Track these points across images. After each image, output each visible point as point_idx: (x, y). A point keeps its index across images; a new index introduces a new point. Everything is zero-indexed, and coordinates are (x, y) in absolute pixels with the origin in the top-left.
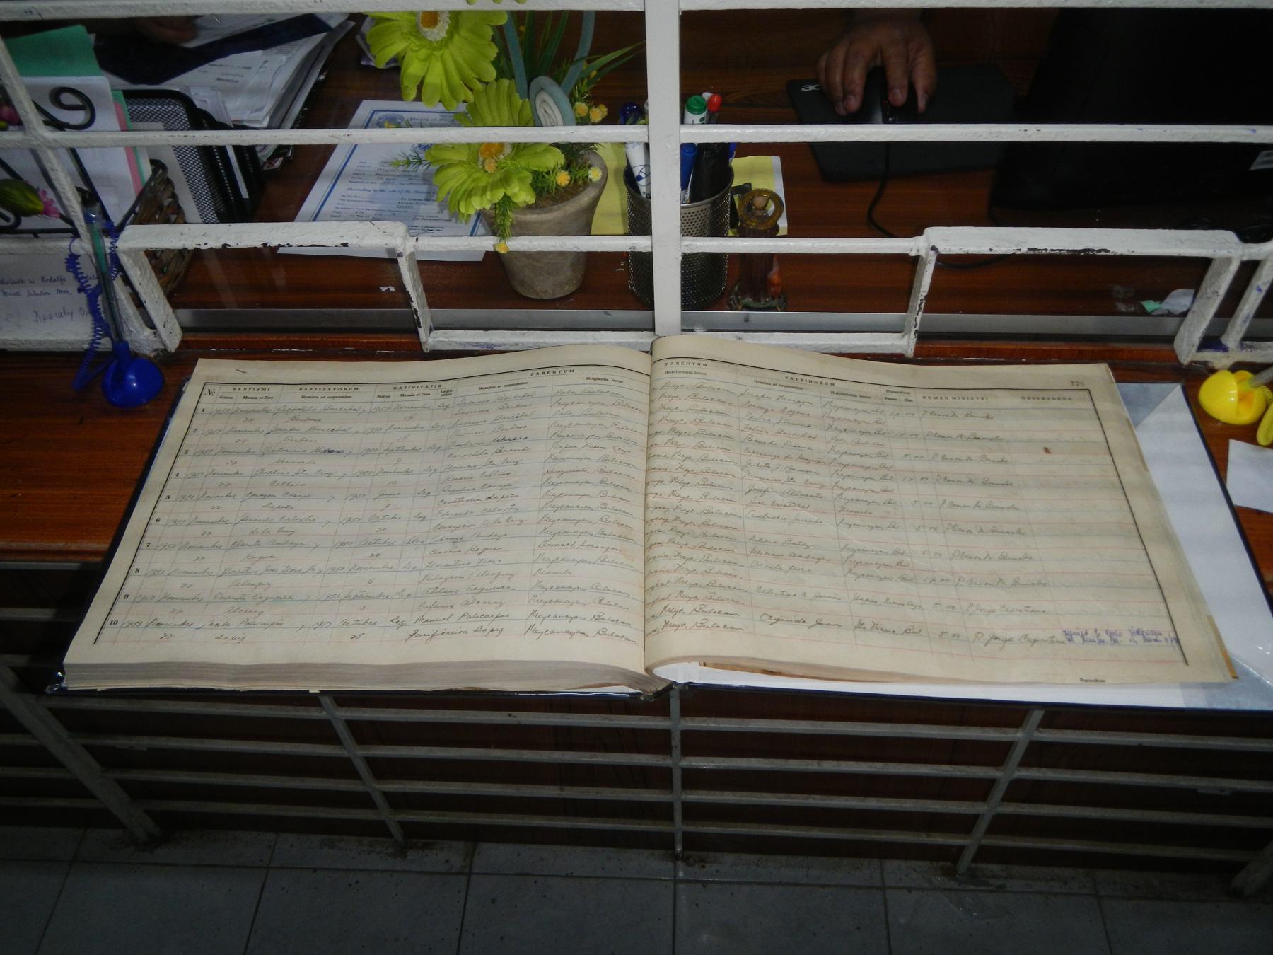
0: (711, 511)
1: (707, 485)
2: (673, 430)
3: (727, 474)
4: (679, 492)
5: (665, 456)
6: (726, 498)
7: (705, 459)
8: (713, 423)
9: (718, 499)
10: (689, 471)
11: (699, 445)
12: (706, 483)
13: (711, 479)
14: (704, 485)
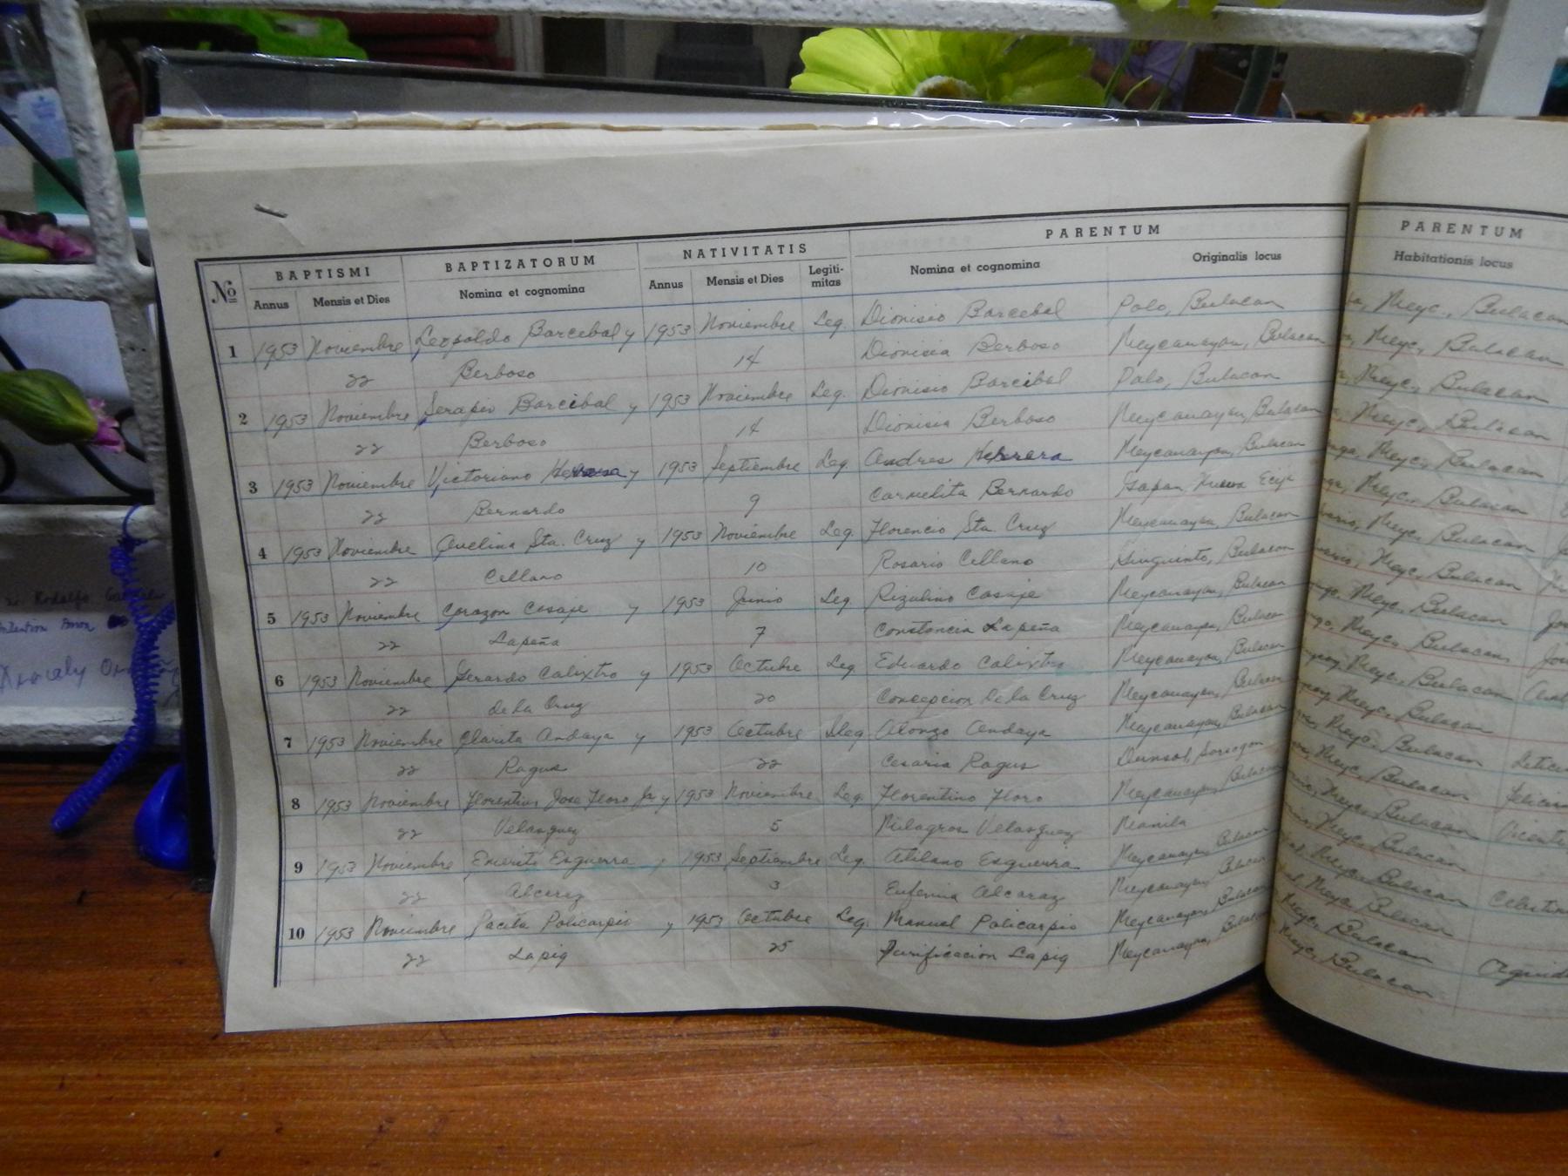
0: (1440, 680)
1: (1444, 612)
2: (1383, 449)
3: (1501, 583)
4: (1367, 624)
5: (1353, 523)
6: (1485, 649)
7: (1453, 539)
8: (1500, 429)
9: (1464, 651)
10: (1401, 572)
11: (1446, 498)
12: (1442, 607)
13: (1458, 595)
14: (1434, 611)
